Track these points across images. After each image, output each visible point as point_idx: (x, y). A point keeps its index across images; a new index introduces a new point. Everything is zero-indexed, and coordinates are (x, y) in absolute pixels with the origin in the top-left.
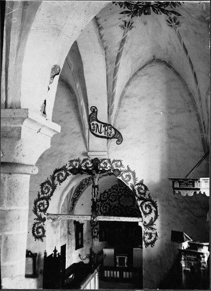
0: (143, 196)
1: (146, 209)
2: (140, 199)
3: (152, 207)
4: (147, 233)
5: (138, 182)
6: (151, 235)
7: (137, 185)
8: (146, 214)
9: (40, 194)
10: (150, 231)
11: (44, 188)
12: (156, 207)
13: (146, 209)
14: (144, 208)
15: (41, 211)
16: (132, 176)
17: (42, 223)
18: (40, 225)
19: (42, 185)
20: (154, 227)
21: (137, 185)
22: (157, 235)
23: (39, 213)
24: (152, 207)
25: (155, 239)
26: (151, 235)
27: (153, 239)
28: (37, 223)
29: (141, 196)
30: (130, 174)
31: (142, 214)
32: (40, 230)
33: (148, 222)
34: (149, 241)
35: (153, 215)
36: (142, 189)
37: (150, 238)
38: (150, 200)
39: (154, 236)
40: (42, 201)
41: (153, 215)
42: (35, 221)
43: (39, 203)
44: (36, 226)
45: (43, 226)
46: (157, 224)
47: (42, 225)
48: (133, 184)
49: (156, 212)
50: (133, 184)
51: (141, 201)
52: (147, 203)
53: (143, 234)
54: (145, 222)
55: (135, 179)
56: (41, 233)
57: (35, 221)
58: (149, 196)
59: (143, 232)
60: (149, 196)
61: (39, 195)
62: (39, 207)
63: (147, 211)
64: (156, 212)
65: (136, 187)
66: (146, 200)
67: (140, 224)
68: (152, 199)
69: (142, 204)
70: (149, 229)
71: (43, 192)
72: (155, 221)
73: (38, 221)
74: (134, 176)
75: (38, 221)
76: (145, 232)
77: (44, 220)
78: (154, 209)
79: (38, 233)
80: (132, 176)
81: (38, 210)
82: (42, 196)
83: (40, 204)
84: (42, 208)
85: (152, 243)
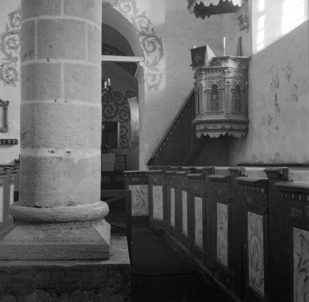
0: (145, 31)
1: (149, 46)
2: (142, 34)
3: (157, 45)
4: (150, 74)
5: (139, 14)
6: (154, 76)
7: (138, 17)
8: (148, 52)
9: (9, 26)
10: (154, 73)
11: (14, 19)
12: (161, 45)
13: (149, 46)
14: (146, 45)
15: (12, 48)
16: (132, 7)
17: (13, 64)
18: (10, 66)
19: (12, 15)
20: (157, 66)
21: (138, 17)
22: (161, 77)
23: (8, 51)
24: (157, 45)
25: (160, 81)
26: (154, 76)
27: (156, 81)
28: (7, 63)
29: (143, 30)
30: (130, 3)
31: (145, 53)
32: (11, 72)
33: (151, 61)
34: (152, 84)
35: (157, 53)
36: (145, 23)
37: (154, 79)
38: (154, 36)
39: (158, 77)
40: (12, 36)
41: (157, 53)
42: (4, 61)
43: (7, 39)
44: (5, 67)
45: (15, 67)
46: (162, 65)
47: (14, 66)
48: (133, 16)
49: (161, 50)
50: (133, 16)
51: (144, 37)
52: (150, 39)
53: (145, 76)
54: (148, 62)
55: (136, 11)
56: (13, 76)
57: (3, 61)
58: (153, 32)
59: (145, 73)
60: (153, 32)
61: (7, 29)
62: (8, 43)
63: (151, 48)
64: (161, 50)
65: (137, 20)
66: (149, 36)
67: (141, 64)
68: (157, 35)
69: (144, 39)
70: (152, 70)
71: (13, 26)
72: (159, 60)
73: (8, 61)
74: (134, 6)
75: (8, 61)
76: (148, 73)
77: (16, 59)
78: (158, 46)
79: (8, 77)
80: (132, 7)
81: (7, 47)
82: (11, 29)
83: (9, 39)
84: (12, 45)
85: (155, 86)
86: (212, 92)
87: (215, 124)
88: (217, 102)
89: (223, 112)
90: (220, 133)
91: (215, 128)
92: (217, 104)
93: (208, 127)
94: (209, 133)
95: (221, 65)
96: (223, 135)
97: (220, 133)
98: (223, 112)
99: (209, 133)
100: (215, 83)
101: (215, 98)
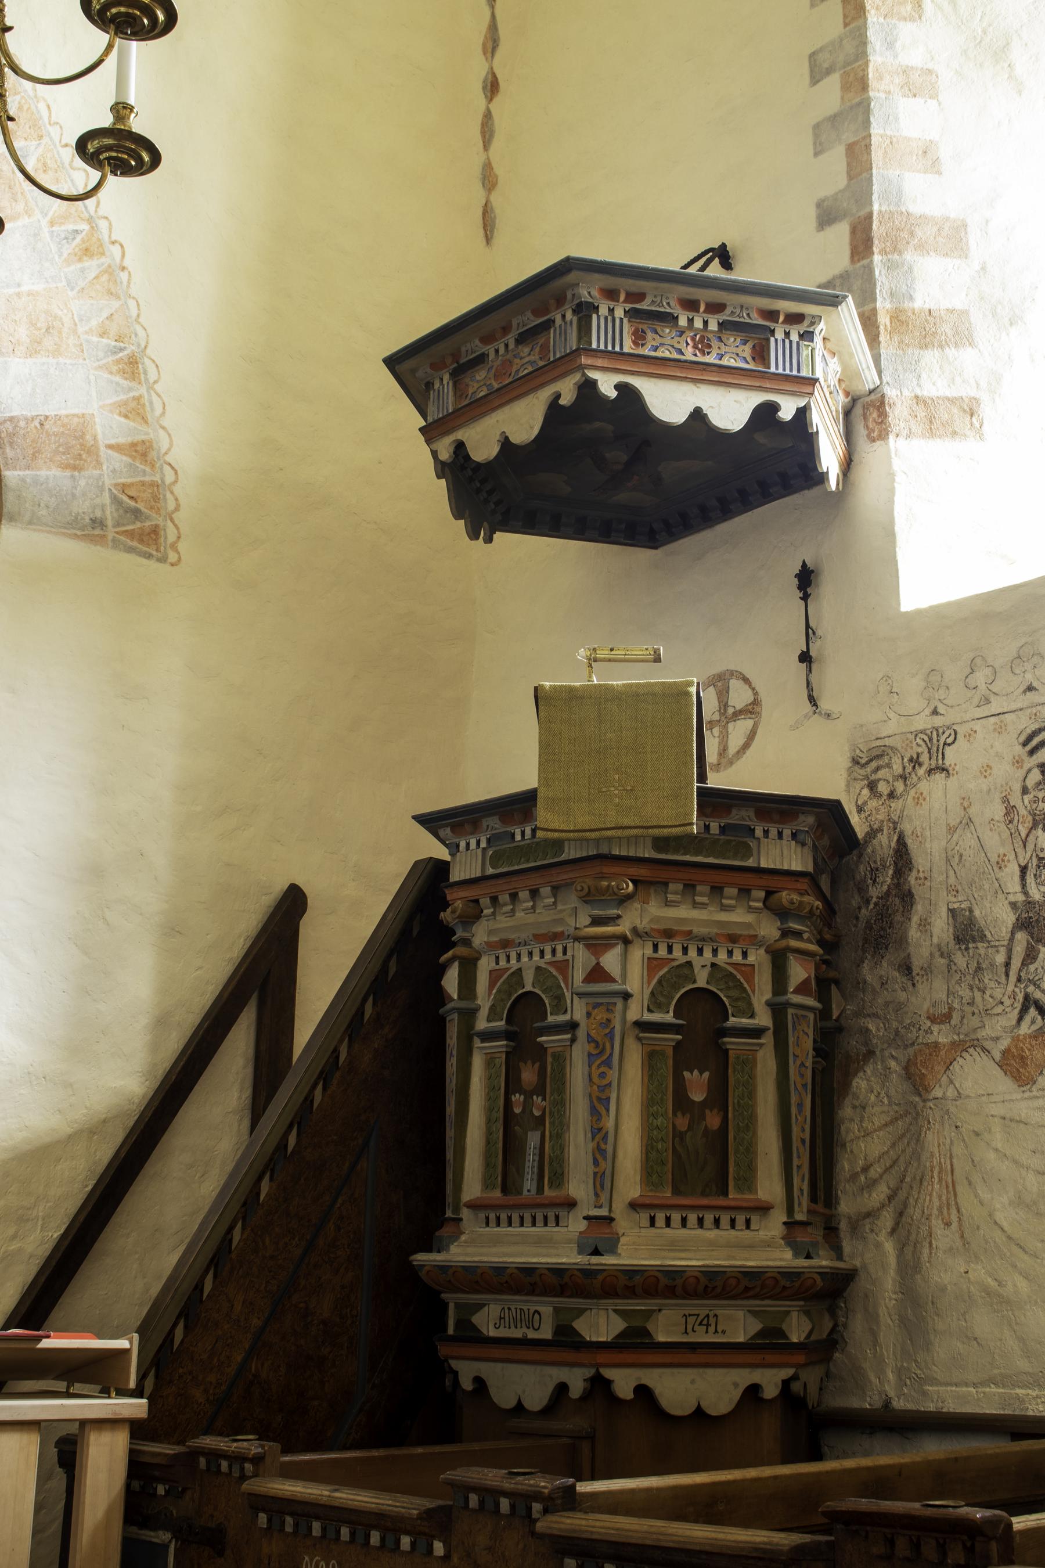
86: (678, 1047)
87: (701, 1307)
88: (713, 1121)
89: (764, 1209)
90: (745, 1377)
91: (701, 1336)
92: (719, 1142)
93: (650, 1327)
94: (654, 1379)
95: (748, 852)
96: (770, 1391)
97: (745, 1377)
98: (764, 1209)
99: (654, 1379)
100: (702, 980)
101: (698, 1096)
